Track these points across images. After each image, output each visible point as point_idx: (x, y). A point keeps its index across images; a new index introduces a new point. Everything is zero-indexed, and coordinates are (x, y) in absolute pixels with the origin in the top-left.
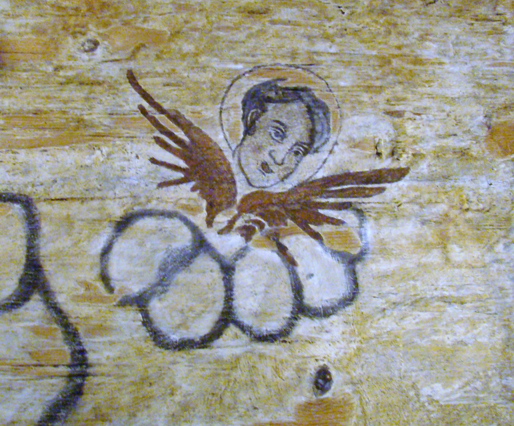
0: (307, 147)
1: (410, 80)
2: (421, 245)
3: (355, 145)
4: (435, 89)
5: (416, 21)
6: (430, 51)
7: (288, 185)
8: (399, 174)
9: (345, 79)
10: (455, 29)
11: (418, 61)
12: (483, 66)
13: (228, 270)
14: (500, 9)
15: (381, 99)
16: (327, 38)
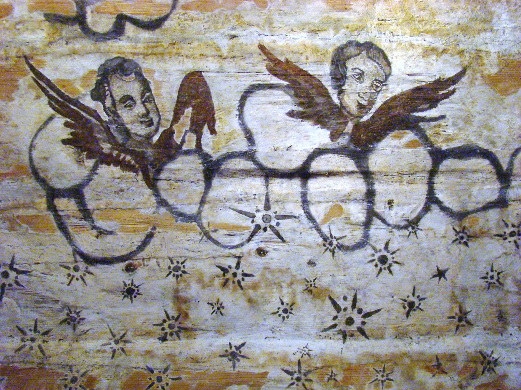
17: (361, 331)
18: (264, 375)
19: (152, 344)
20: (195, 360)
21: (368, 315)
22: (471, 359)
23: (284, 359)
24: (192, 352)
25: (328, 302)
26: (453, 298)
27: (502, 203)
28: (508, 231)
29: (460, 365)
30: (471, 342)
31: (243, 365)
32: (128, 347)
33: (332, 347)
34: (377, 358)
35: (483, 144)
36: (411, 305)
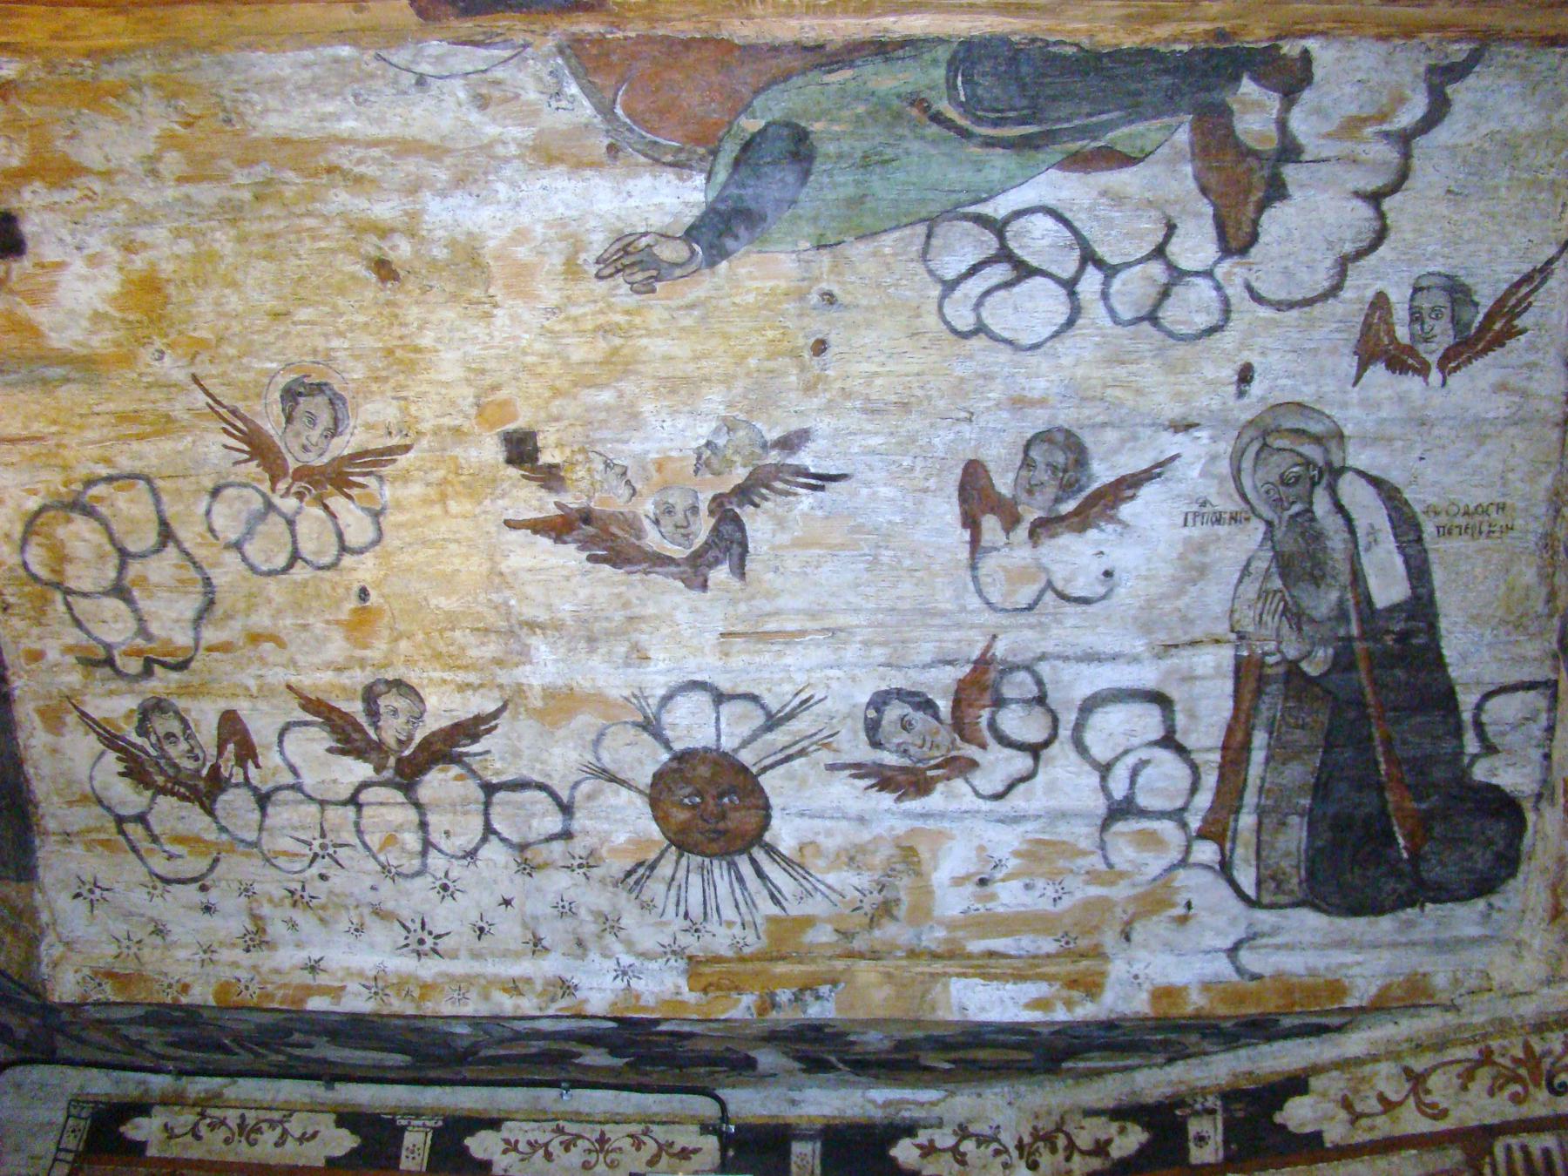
0: (334, 431)
1: (410, 368)
2: (427, 502)
3: (369, 427)
4: (433, 375)
5: (415, 310)
6: (427, 340)
7: (326, 459)
8: (407, 448)
9: (358, 372)
10: (449, 314)
11: (417, 350)
12: (475, 350)
13: (291, 523)
14: (492, 291)
15: (388, 387)
16: (341, 334)
17: (435, 951)
18: (343, 988)
19: (238, 954)
20: (277, 971)
21: (439, 936)
22: (549, 983)
23: (361, 974)
24: (274, 964)
25: (397, 925)
26: (525, 925)
27: (567, 835)
28: (577, 862)
29: (539, 988)
30: (550, 966)
31: (323, 979)
32: (215, 957)
33: (405, 963)
34: (452, 978)
35: (537, 778)
36: (481, 929)
